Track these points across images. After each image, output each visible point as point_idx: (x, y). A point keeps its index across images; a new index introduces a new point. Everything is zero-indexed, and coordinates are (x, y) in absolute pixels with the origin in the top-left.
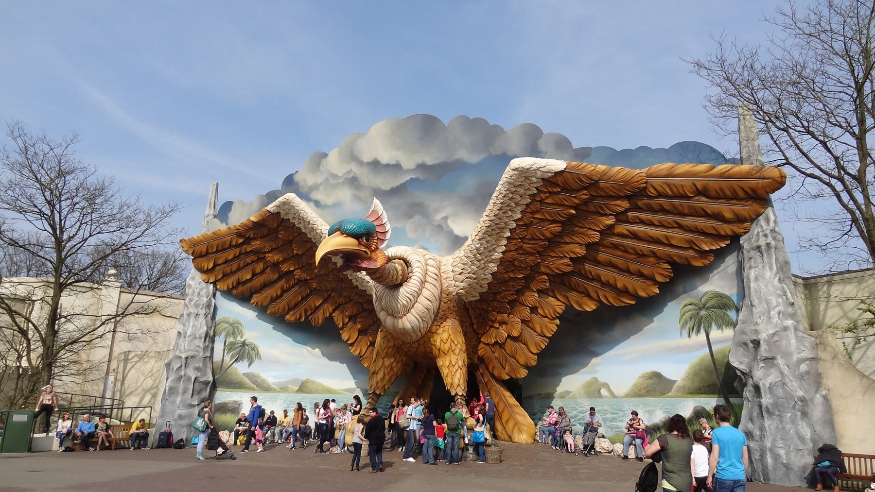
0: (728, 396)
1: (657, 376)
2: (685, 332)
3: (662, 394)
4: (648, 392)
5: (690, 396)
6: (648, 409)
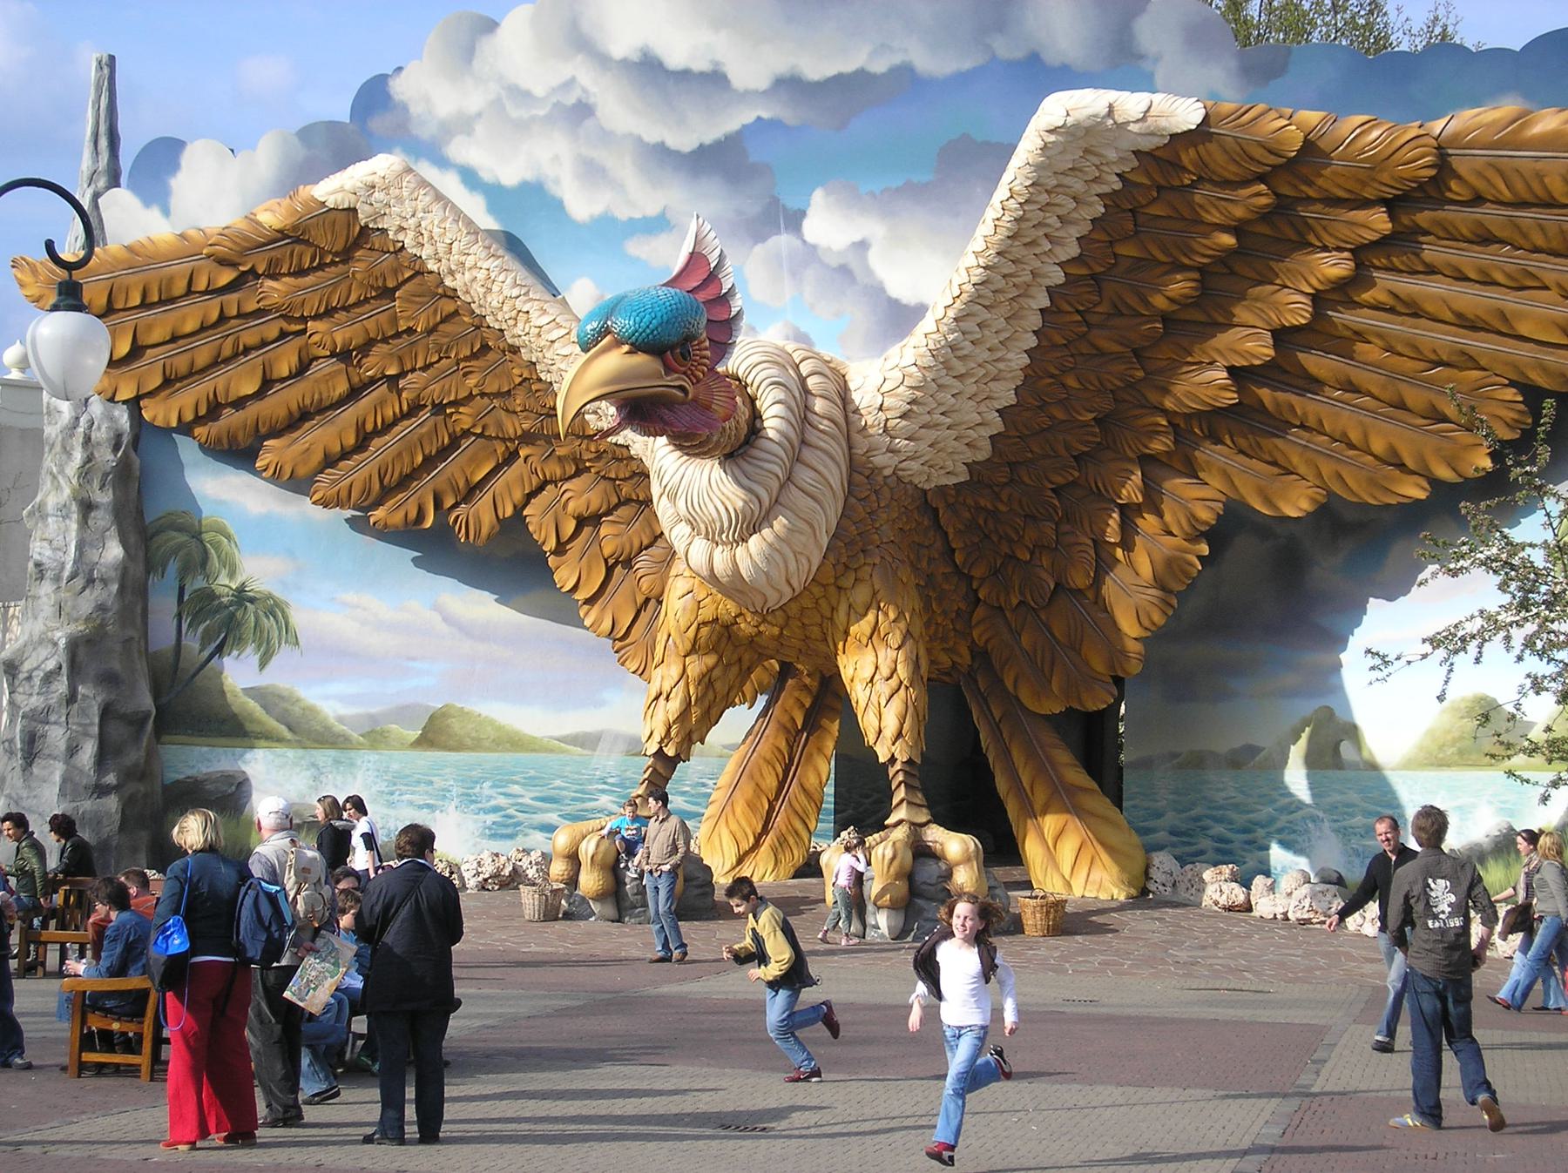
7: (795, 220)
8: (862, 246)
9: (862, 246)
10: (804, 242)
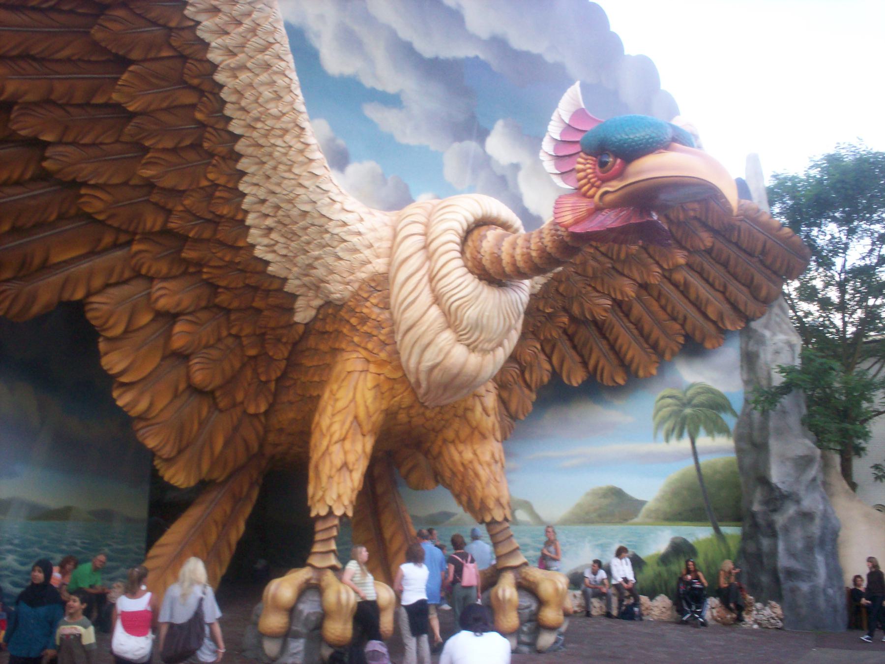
0: (719, 523)
1: (617, 494)
2: (661, 435)
3: (624, 519)
4: (600, 516)
5: (666, 523)
6: (600, 542)
7: (482, 135)
8: (516, 167)
9: (516, 167)
10: (485, 152)
